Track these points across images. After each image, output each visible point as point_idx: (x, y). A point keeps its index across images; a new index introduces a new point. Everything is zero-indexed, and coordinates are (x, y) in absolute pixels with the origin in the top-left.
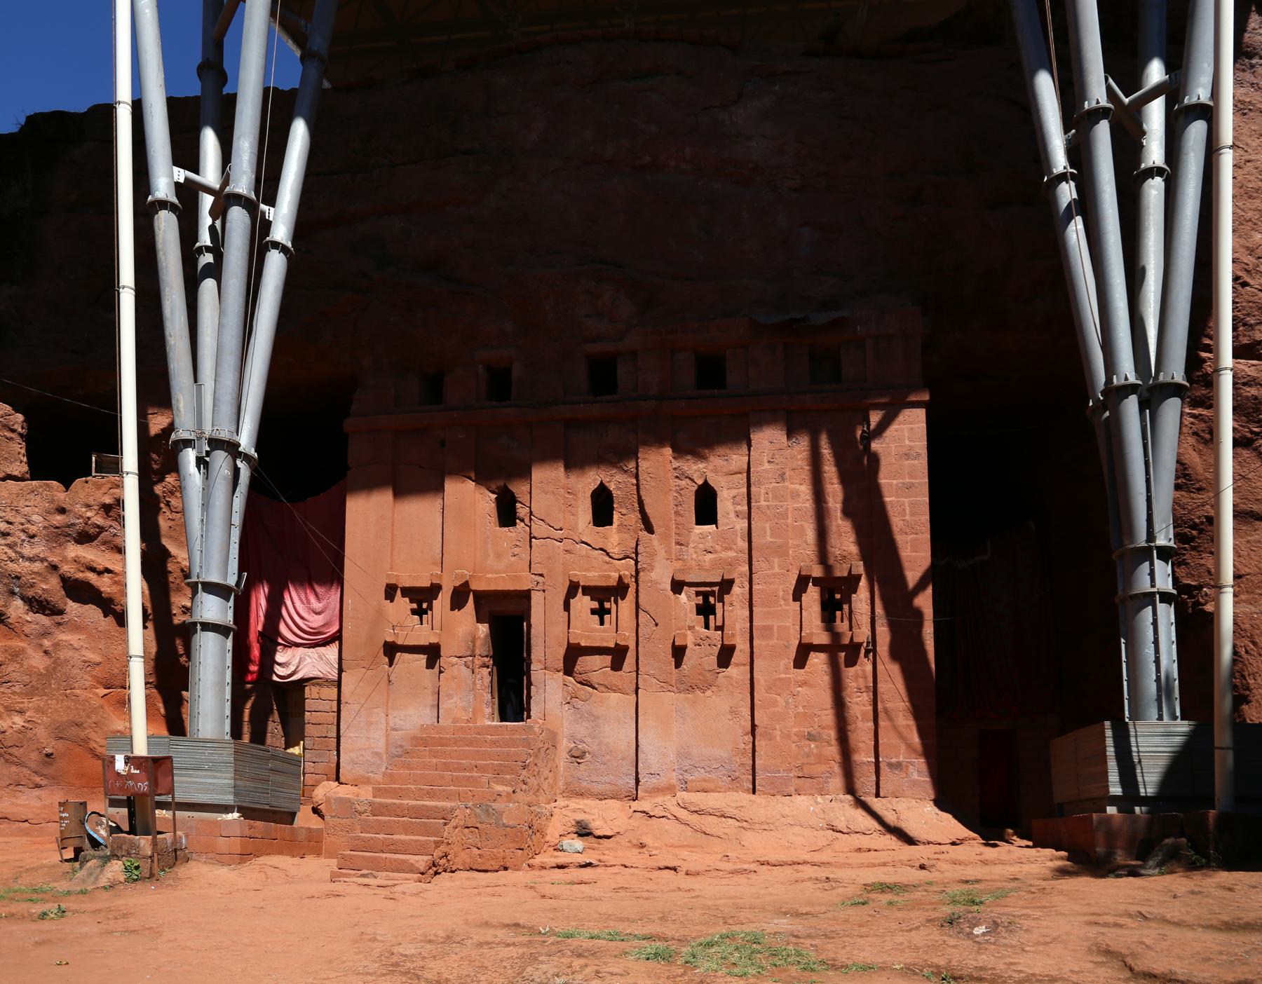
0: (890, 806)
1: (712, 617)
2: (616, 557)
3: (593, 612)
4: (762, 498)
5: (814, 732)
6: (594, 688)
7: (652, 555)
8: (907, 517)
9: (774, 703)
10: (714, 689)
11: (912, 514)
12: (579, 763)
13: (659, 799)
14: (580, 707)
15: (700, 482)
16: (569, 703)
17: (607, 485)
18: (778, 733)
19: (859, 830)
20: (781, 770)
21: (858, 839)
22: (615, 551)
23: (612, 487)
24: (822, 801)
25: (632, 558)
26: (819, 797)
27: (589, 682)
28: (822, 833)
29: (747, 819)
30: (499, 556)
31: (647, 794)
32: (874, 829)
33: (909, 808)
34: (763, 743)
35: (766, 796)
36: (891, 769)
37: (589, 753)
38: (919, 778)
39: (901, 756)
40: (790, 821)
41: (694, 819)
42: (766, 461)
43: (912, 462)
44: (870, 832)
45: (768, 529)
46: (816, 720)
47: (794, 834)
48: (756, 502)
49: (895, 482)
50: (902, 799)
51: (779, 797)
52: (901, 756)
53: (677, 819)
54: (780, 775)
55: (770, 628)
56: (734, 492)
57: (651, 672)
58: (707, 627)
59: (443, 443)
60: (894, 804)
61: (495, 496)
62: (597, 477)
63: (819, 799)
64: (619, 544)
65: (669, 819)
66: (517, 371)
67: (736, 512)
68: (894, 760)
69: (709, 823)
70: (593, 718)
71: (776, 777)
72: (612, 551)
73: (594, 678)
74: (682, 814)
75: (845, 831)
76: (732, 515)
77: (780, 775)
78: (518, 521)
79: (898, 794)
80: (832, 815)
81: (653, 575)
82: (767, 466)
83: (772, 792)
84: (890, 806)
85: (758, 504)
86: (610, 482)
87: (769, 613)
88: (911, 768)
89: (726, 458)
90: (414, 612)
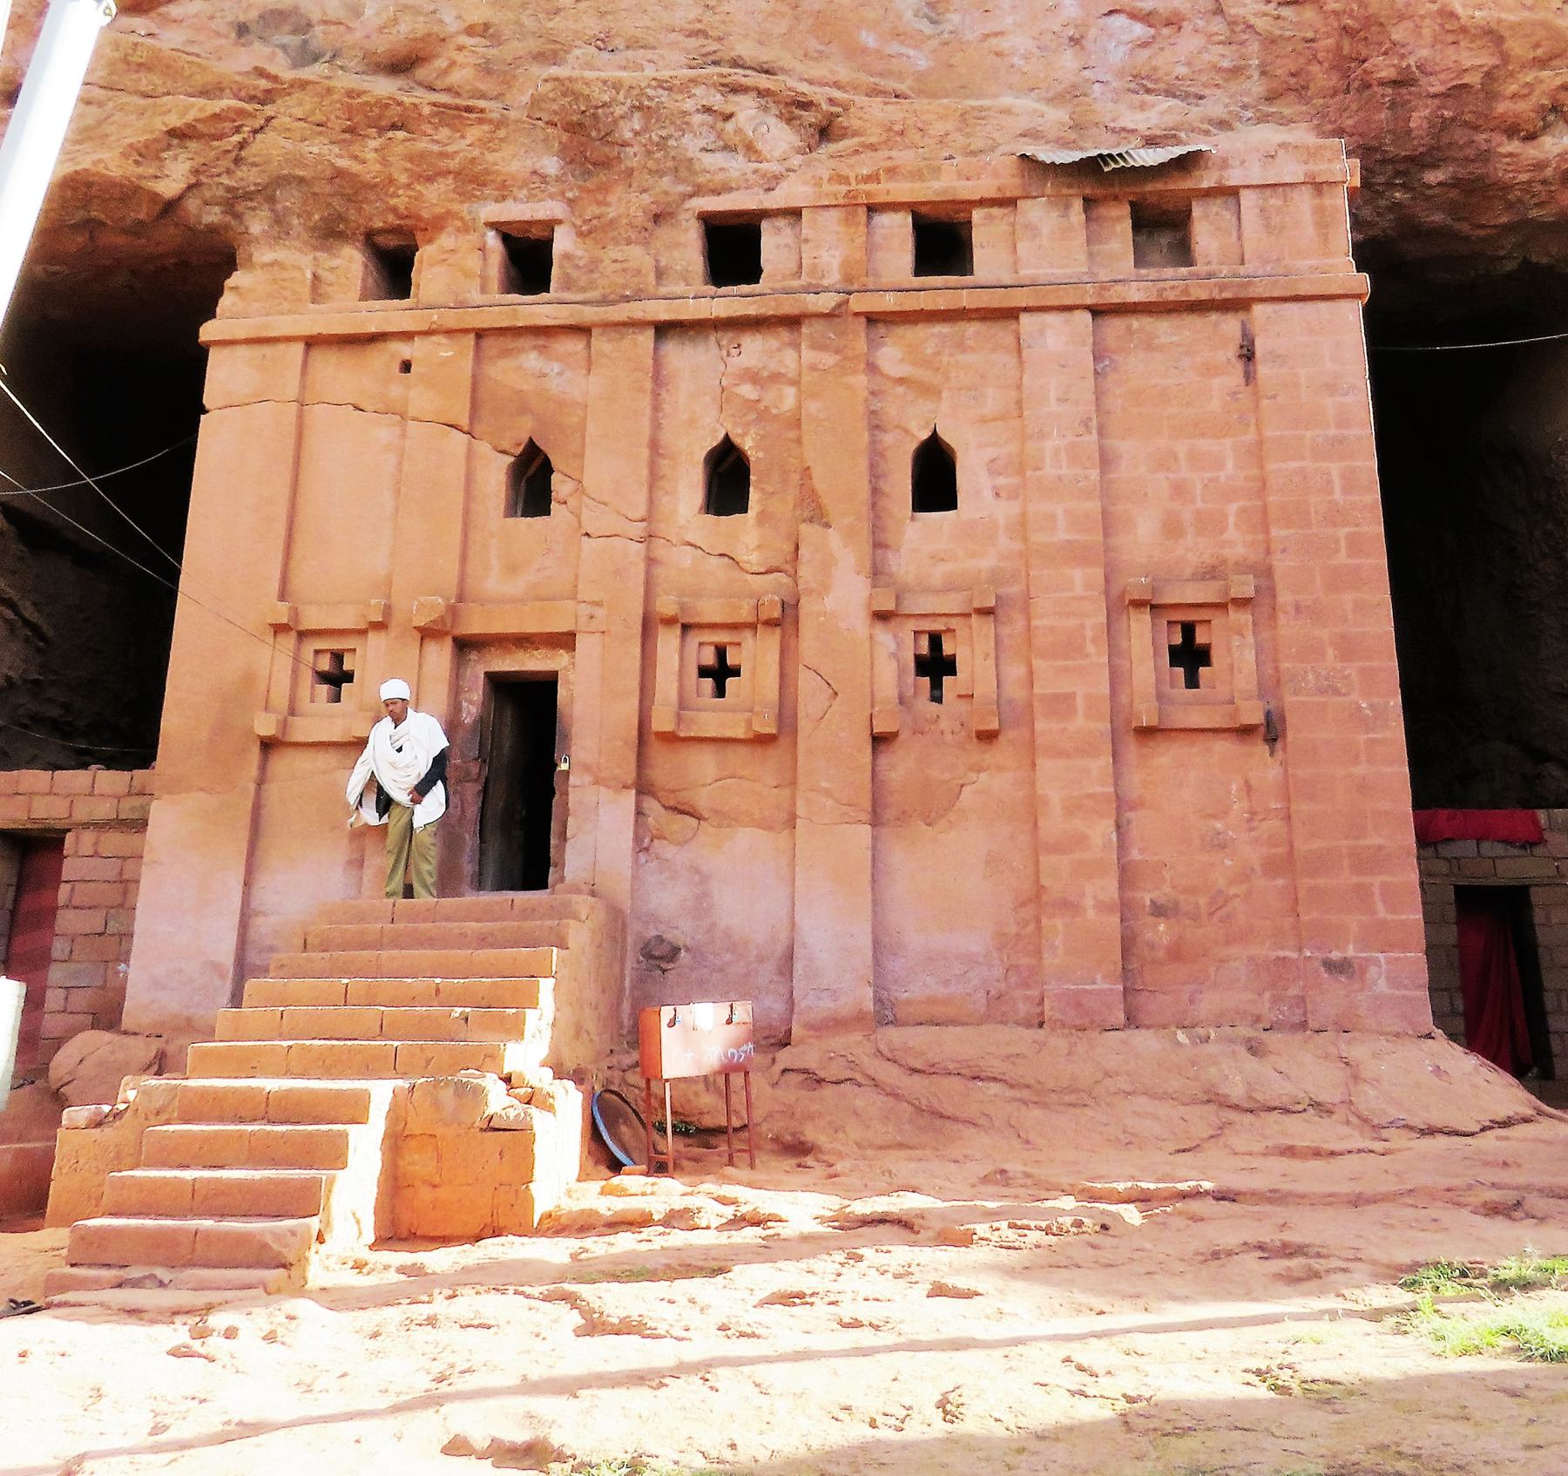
0: (1332, 1050)
1: (947, 680)
2: (755, 569)
3: (704, 672)
4: (1048, 462)
5: (1162, 901)
6: (699, 818)
7: (827, 565)
8: (1338, 495)
9: (1080, 841)
10: (952, 816)
11: (1347, 490)
12: (664, 971)
13: (838, 1042)
14: (669, 856)
15: (925, 435)
16: (647, 849)
17: (737, 440)
18: (1089, 902)
19: (1277, 1104)
20: (1099, 977)
21: (1276, 1122)
22: (753, 559)
23: (747, 444)
24: (1187, 1042)
25: (785, 572)
26: (1179, 1032)
27: (691, 806)
28: (1191, 1112)
29: (1032, 1082)
30: (512, 569)
31: (811, 1033)
32: (1307, 1101)
33: (1376, 1055)
34: (1059, 923)
35: (1066, 1031)
36: (1330, 973)
37: (688, 950)
38: (1391, 991)
39: (1351, 947)
40: (1123, 1083)
41: (916, 1084)
42: (1053, 395)
43: (1340, 399)
44: (1300, 1108)
45: (1060, 516)
46: (1167, 876)
47: (1134, 1112)
48: (1037, 469)
49: (1309, 434)
50: (1357, 1034)
51: (1095, 1034)
52: (1351, 947)
53: (876, 1084)
54: (1094, 986)
55: (1069, 698)
56: (990, 453)
57: (824, 784)
58: (937, 699)
59: (406, 367)
60: (1343, 1046)
61: (512, 459)
62: (718, 426)
63: (1181, 1037)
64: (759, 547)
65: (860, 1085)
66: (563, 242)
67: (994, 487)
68: (1336, 955)
69: (947, 1093)
70: (697, 878)
71: (1086, 991)
72: (745, 558)
73: (703, 799)
74: (890, 1074)
75: (1246, 1105)
76: (988, 494)
77: (1094, 986)
78: (553, 505)
79: (1348, 1027)
80: (1213, 1070)
81: (829, 603)
82: (1053, 406)
83: (1078, 1022)
84: (1332, 1050)
85: (1039, 473)
86: (744, 435)
87: (1066, 669)
88: (1373, 970)
89: (973, 393)
90: (324, 678)
